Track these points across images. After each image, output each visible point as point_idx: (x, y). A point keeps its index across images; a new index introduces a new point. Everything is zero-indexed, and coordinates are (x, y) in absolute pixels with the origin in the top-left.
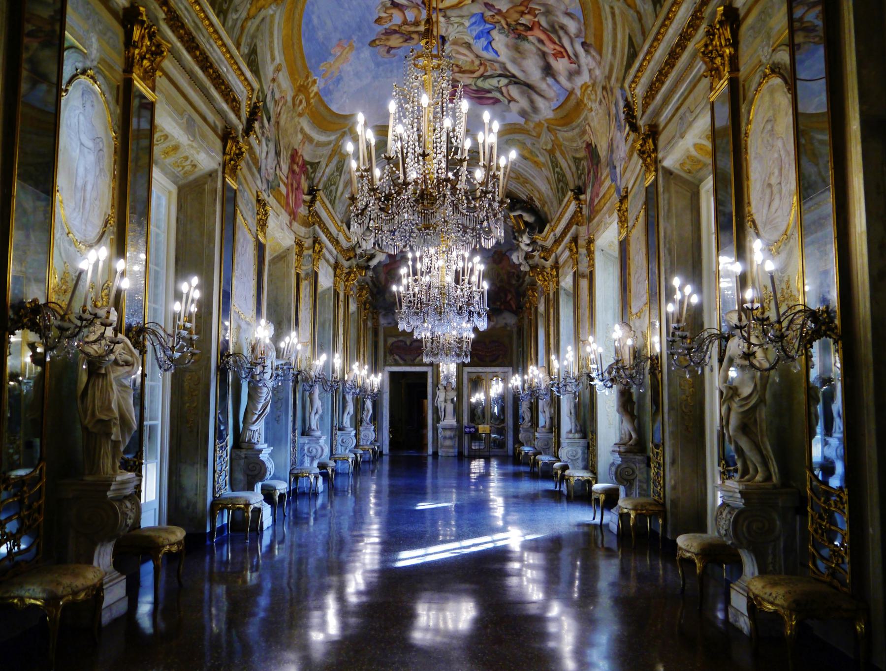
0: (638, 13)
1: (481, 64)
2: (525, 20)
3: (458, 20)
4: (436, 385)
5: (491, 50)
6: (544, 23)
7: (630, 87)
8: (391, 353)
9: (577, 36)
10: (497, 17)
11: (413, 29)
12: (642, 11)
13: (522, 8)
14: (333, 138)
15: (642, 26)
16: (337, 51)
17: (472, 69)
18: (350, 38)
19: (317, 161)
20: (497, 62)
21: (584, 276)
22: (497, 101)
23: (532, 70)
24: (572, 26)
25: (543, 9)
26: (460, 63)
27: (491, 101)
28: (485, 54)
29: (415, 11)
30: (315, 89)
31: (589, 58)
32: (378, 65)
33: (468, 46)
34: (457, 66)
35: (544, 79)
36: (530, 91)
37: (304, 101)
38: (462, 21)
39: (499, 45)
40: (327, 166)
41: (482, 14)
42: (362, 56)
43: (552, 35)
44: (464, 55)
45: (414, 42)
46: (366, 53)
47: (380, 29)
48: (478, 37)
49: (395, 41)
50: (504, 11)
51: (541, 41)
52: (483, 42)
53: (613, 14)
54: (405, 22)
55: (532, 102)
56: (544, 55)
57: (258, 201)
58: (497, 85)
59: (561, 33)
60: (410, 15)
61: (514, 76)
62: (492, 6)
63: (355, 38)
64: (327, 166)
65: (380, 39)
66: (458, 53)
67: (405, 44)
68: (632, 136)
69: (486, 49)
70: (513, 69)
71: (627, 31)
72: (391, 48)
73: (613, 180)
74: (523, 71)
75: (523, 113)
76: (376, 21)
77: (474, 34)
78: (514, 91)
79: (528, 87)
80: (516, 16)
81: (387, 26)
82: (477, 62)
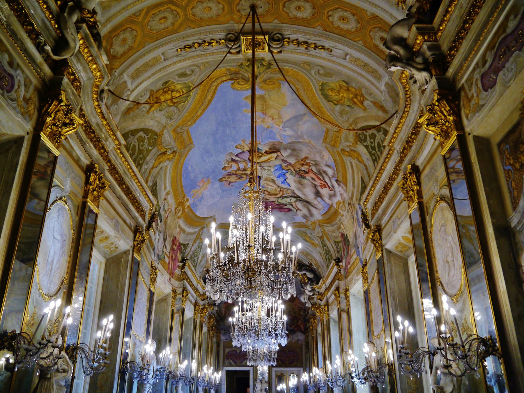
0: (365, 165)
1: (281, 191)
3: (268, 168)
4: (255, 379)
5: (286, 183)
7: (364, 204)
8: (228, 359)
9: (333, 177)
10: (289, 167)
11: (243, 172)
12: (367, 164)
13: (303, 162)
14: (197, 230)
15: (368, 172)
16: (201, 184)
17: (276, 193)
18: (208, 177)
19: (187, 243)
21: (344, 311)
22: (290, 210)
23: (309, 194)
24: (330, 172)
25: (314, 163)
26: (269, 190)
28: (283, 186)
29: (244, 164)
30: (188, 204)
31: (340, 188)
32: (223, 191)
33: (274, 181)
34: (267, 191)
35: (316, 198)
36: (308, 205)
37: (181, 210)
38: (270, 168)
39: (290, 181)
40: (193, 246)
41: (281, 165)
42: (215, 186)
43: (319, 176)
44: (271, 186)
45: (243, 179)
46: (217, 184)
47: (225, 172)
48: (279, 177)
49: (233, 178)
50: (293, 164)
52: (282, 179)
53: (352, 166)
54: (239, 169)
55: (309, 211)
56: (315, 186)
57: (152, 267)
59: (324, 175)
60: (242, 166)
61: (299, 197)
62: (286, 161)
63: (211, 177)
64: (193, 246)
66: (268, 185)
68: (367, 231)
69: (283, 183)
71: (360, 175)
73: (358, 255)
74: (304, 194)
75: (305, 217)
76: (223, 169)
77: (277, 175)
78: (299, 205)
80: (299, 166)
81: (229, 171)
82: (278, 190)
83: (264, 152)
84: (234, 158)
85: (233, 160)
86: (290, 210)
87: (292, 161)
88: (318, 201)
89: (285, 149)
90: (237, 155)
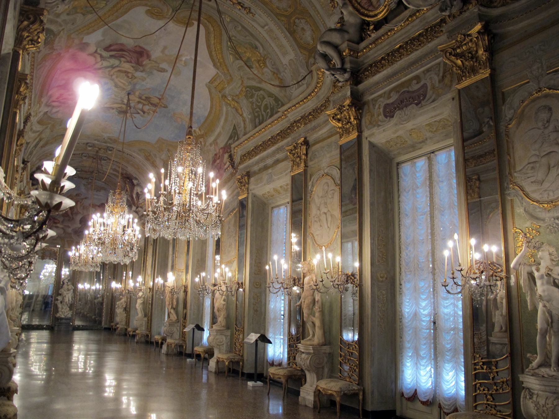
26: (126, 78)
27: (112, 48)
34: (128, 77)
45: (145, 96)
46: (172, 106)
47: (158, 110)
49: (156, 101)
54: (144, 105)
58: (104, 62)
60: (140, 106)
65: (161, 106)
67: (151, 96)
72: (160, 99)
84: (142, 113)
85: (144, 112)
86: (107, 49)
90: (139, 113)
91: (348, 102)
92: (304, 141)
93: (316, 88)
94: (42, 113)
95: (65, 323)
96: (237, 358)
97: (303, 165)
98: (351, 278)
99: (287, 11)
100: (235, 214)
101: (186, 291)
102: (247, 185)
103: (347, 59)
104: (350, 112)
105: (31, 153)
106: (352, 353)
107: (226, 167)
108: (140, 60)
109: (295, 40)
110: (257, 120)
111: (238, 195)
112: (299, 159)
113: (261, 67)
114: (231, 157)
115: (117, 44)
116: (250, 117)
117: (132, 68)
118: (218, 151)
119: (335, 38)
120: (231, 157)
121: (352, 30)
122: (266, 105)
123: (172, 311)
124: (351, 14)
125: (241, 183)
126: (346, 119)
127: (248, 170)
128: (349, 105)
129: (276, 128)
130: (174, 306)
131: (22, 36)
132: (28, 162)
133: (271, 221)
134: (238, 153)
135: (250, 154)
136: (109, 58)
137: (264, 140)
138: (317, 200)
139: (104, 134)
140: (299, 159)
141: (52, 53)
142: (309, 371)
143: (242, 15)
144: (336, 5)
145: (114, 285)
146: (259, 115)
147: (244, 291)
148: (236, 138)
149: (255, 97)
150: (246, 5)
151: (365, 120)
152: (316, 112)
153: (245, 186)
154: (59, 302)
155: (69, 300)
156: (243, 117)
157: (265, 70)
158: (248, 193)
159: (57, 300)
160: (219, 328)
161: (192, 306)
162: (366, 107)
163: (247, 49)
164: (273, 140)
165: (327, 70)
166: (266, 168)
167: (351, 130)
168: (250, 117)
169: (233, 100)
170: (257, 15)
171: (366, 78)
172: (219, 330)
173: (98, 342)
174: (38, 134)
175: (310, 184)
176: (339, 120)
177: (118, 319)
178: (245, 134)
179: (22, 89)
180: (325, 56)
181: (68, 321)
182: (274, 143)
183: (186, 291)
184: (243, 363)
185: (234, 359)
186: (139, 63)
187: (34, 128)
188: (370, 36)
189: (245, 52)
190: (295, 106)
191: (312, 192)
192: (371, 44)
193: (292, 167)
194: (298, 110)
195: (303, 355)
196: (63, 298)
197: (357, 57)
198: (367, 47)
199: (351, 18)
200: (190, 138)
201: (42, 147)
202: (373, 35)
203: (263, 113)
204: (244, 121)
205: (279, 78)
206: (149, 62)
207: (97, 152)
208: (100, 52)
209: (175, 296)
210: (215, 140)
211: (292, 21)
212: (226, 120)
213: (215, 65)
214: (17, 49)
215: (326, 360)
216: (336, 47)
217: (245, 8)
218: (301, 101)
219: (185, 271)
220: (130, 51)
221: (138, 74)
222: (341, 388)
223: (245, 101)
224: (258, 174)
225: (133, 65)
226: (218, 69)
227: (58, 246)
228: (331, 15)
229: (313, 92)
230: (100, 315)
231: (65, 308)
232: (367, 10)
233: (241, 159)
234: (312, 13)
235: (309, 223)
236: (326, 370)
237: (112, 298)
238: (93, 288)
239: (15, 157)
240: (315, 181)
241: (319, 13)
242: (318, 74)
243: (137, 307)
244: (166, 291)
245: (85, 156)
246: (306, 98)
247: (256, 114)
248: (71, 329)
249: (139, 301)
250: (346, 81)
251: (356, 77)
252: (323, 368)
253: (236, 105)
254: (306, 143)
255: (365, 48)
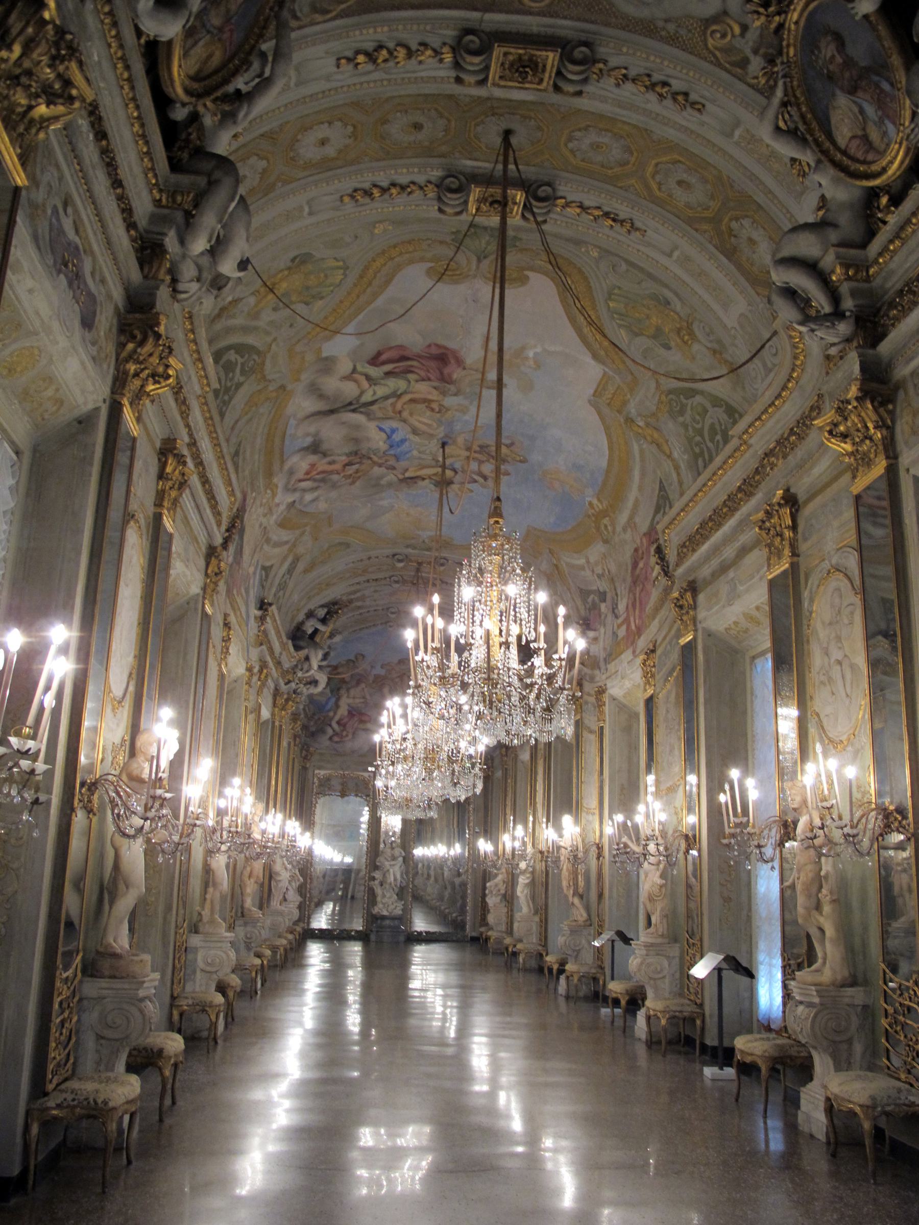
1: (400, 412)
2: (351, 470)
5: (388, 430)
6: (335, 477)
17: (413, 405)
20: (379, 419)
22: (375, 361)
23: (332, 433)
24: (309, 497)
26: (428, 413)
27: (384, 357)
28: (394, 424)
33: (415, 432)
34: (433, 410)
36: (327, 408)
44: (420, 422)
46: (535, 457)
48: (403, 441)
51: (330, 463)
52: (397, 437)
54: (481, 462)
55: (321, 396)
56: (325, 455)
58: (376, 388)
61: (354, 411)
62: (387, 468)
69: (393, 431)
70: (359, 418)
74: (344, 423)
75: (327, 365)
77: (407, 444)
78: (349, 390)
79: (333, 409)
82: (405, 414)
83: (427, 481)
84: (481, 480)
85: (485, 478)
86: (375, 361)
87: (377, 471)
88: (308, 435)
89: (390, 485)
90: (475, 481)
91: (853, 391)
92: (783, 498)
93: (793, 370)
94: (282, 507)
95: (390, 927)
96: (689, 1009)
97: (787, 552)
98: (896, 819)
99: (707, 209)
100: (677, 677)
101: (599, 856)
102: (691, 613)
103: (844, 289)
104: (863, 414)
105: (282, 587)
106: (909, 1009)
107: (655, 574)
108: (446, 371)
109: (739, 267)
110: (700, 461)
111: (679, 635)
112: (779, 539)
113: (686, 343)
114: (659, 550)
115: (391, 348)
116: (686, 457)
117: (435, 392)
118: (638, 541)
119: (807, 246)
120: (659, 550)
121: (844, 219)
122: (712, 424)
123: (576, 901)
124: (836, 181)
125: (681, 607)
126: (858, 430)
127: (690, 579)
128: (857, 399)
129: (733, 477)
130: (581, 890)
131: (126, 373)
132: (270, 605)
133: (752, 688)
134: (672, 540)
135: (692, 542)
136: (382, 379)
137: (715, 505)
138: (823, 633)
139: (420, 533)
140: (779, 539)
141: (266, 387)
142: (815, 1048)
143: (620, 238)
144: (806, 169)
145: (484, 846)
146: (702, 453)
147: (699, 851)
148: (667, 508)
149: (689, 411)
150: (622, 216)
151: (902, 428)
152: (801, 427)
153: (687, 613)
154: (377, 882)
155: (395, 880)
156: (673, 460)
157: (696, 347)
158: (696, 630)
159: (374, 879)
160: (650, 940)
161: (615, 890)
162: (901, 394)
163: (649, 309)
164: (731, 504)
165: (801, 323)
166: (724, 569)
167: (872, 456)
168: (686, 457)
169: (648, 425)
170: (649, 233)
171: (893, 325)
172: (652, 945)
173: (460, 967)
174: (286, 547)
175: (806, 594)
176: (844, 436)
177: (491, 919)
178: (682, 494)
179: (169, 469)
180: (790, 293)
181: (396, 922)
182: (733, 510)
183: (599, 856)
184: (703, 1021)
185: (681, 1012)
186: (445, 379)
187: (275, 538)
188: (885, 223)
189: (648, 317)
190: (759, 418)
191: (811, 613)
192: (891, 241)
193: (769, 559)
194: (770, 424)
195: (801, 1008)
196: (384, 875)
197: (868, 279)
198: (885, 249)
199: (841, 192)
200: (497, 522)
201: (306, 571)
202: (893, 219)
203: (710, 444)
204: (677, 468)
205: (726, 361)
206: (464, 373)
207: (418, 570)
208: (364, 370)
209: (581, 868)
210: (631, 518)
211: (724, 228)
212: (643, 474)
213: (595, 356)
214: (117, 397)
215: (855, 1021)
216: (811, 267)
217: (622, 222)
218: (770, 406)
219: (597, 812)
220: (419, 356)
221: (449, 401)
222: (873, 1098)
223: (671, 425)
224: (710, 583)
225: (436, 384)
226: (603, 363)
227: (370, 769)
228: (802, 193)
229: (789, 380)
230: (463, 911)
231: (388, 895)
232: (864, 162)
233: (678, 554)
234: (760, 198)
235: (809, 689)
236: (858, 1048)
237: (482, 872)
238: (452, 853)
239: (204, 598)
240: (814, 590)
241: (775, 197)
242: (791, 337)
243: (519, 894)
244: (562, 858)
245: (397, 582)
246: (779, 396)
247: (697, 450)
248: (402, 938)
249: (522, 880)
250: (848, 340)
251: (871, 324)
252: (850, 1042)
253: (656, 435)
254: (791, 500)
255: (880, 254)
